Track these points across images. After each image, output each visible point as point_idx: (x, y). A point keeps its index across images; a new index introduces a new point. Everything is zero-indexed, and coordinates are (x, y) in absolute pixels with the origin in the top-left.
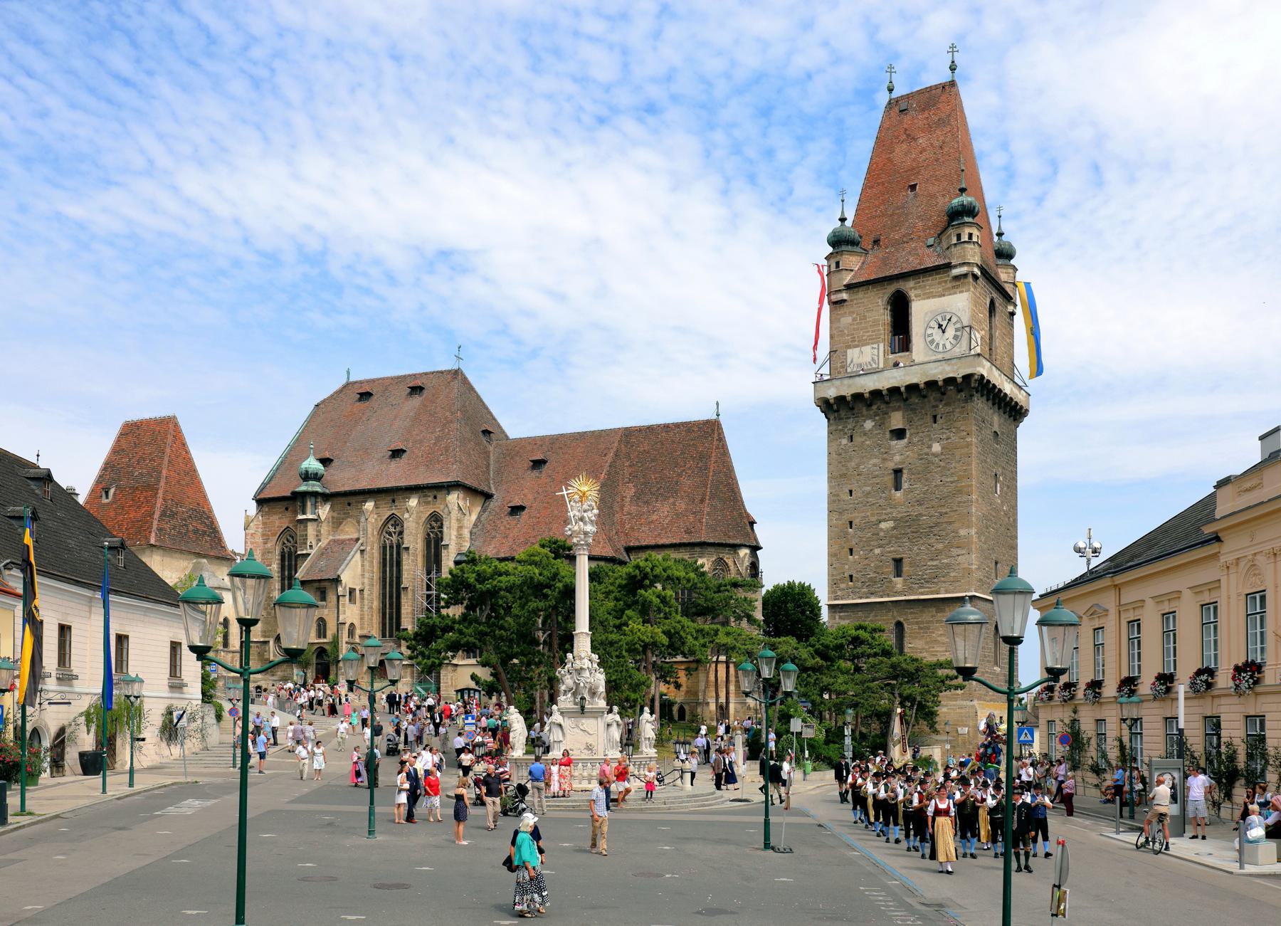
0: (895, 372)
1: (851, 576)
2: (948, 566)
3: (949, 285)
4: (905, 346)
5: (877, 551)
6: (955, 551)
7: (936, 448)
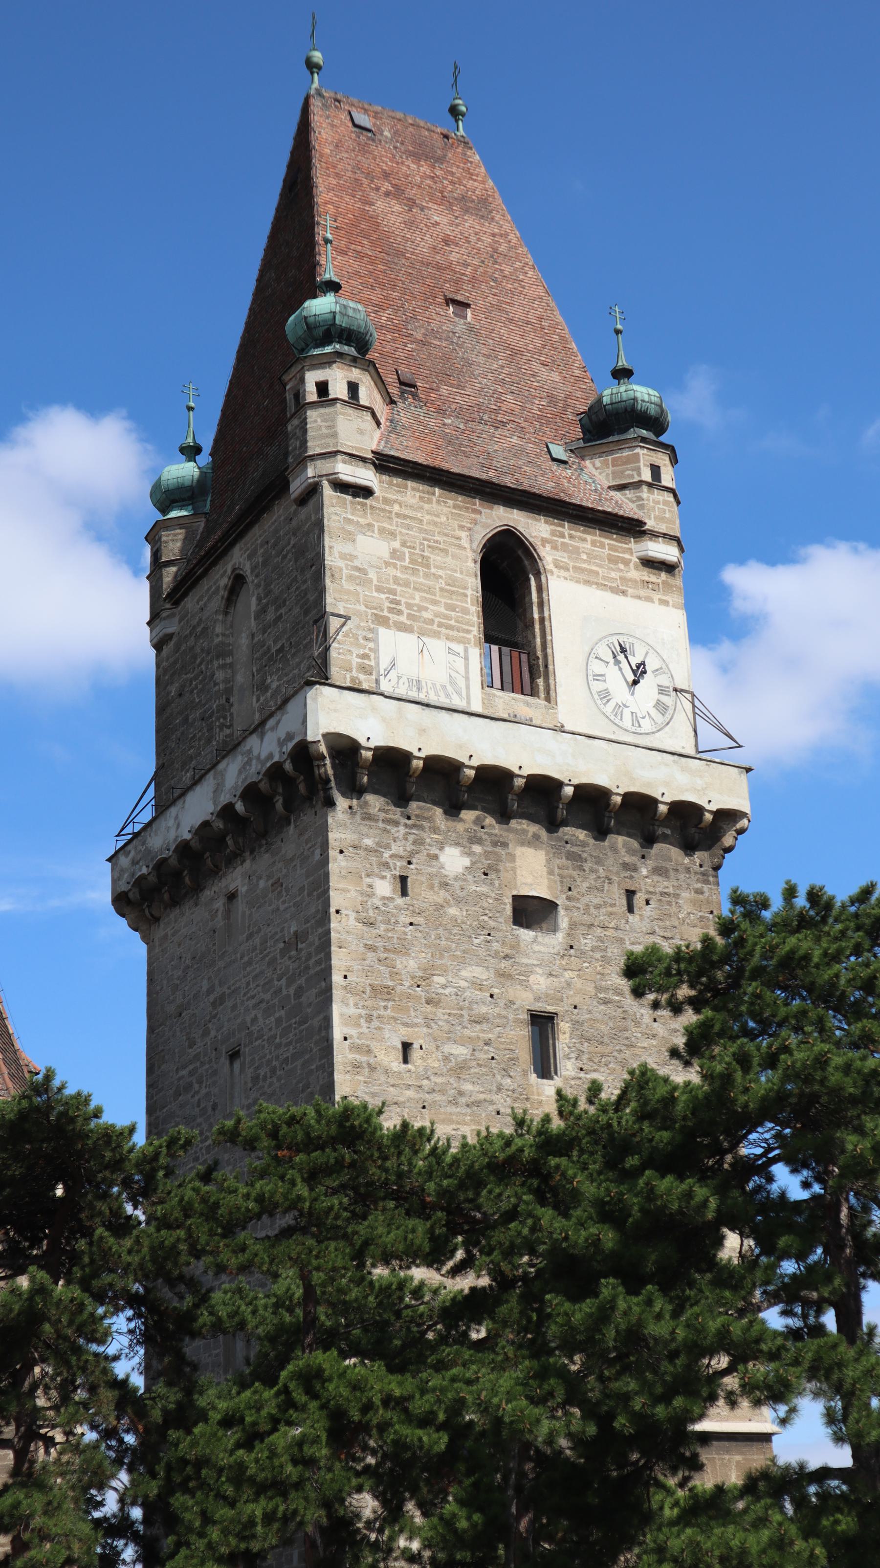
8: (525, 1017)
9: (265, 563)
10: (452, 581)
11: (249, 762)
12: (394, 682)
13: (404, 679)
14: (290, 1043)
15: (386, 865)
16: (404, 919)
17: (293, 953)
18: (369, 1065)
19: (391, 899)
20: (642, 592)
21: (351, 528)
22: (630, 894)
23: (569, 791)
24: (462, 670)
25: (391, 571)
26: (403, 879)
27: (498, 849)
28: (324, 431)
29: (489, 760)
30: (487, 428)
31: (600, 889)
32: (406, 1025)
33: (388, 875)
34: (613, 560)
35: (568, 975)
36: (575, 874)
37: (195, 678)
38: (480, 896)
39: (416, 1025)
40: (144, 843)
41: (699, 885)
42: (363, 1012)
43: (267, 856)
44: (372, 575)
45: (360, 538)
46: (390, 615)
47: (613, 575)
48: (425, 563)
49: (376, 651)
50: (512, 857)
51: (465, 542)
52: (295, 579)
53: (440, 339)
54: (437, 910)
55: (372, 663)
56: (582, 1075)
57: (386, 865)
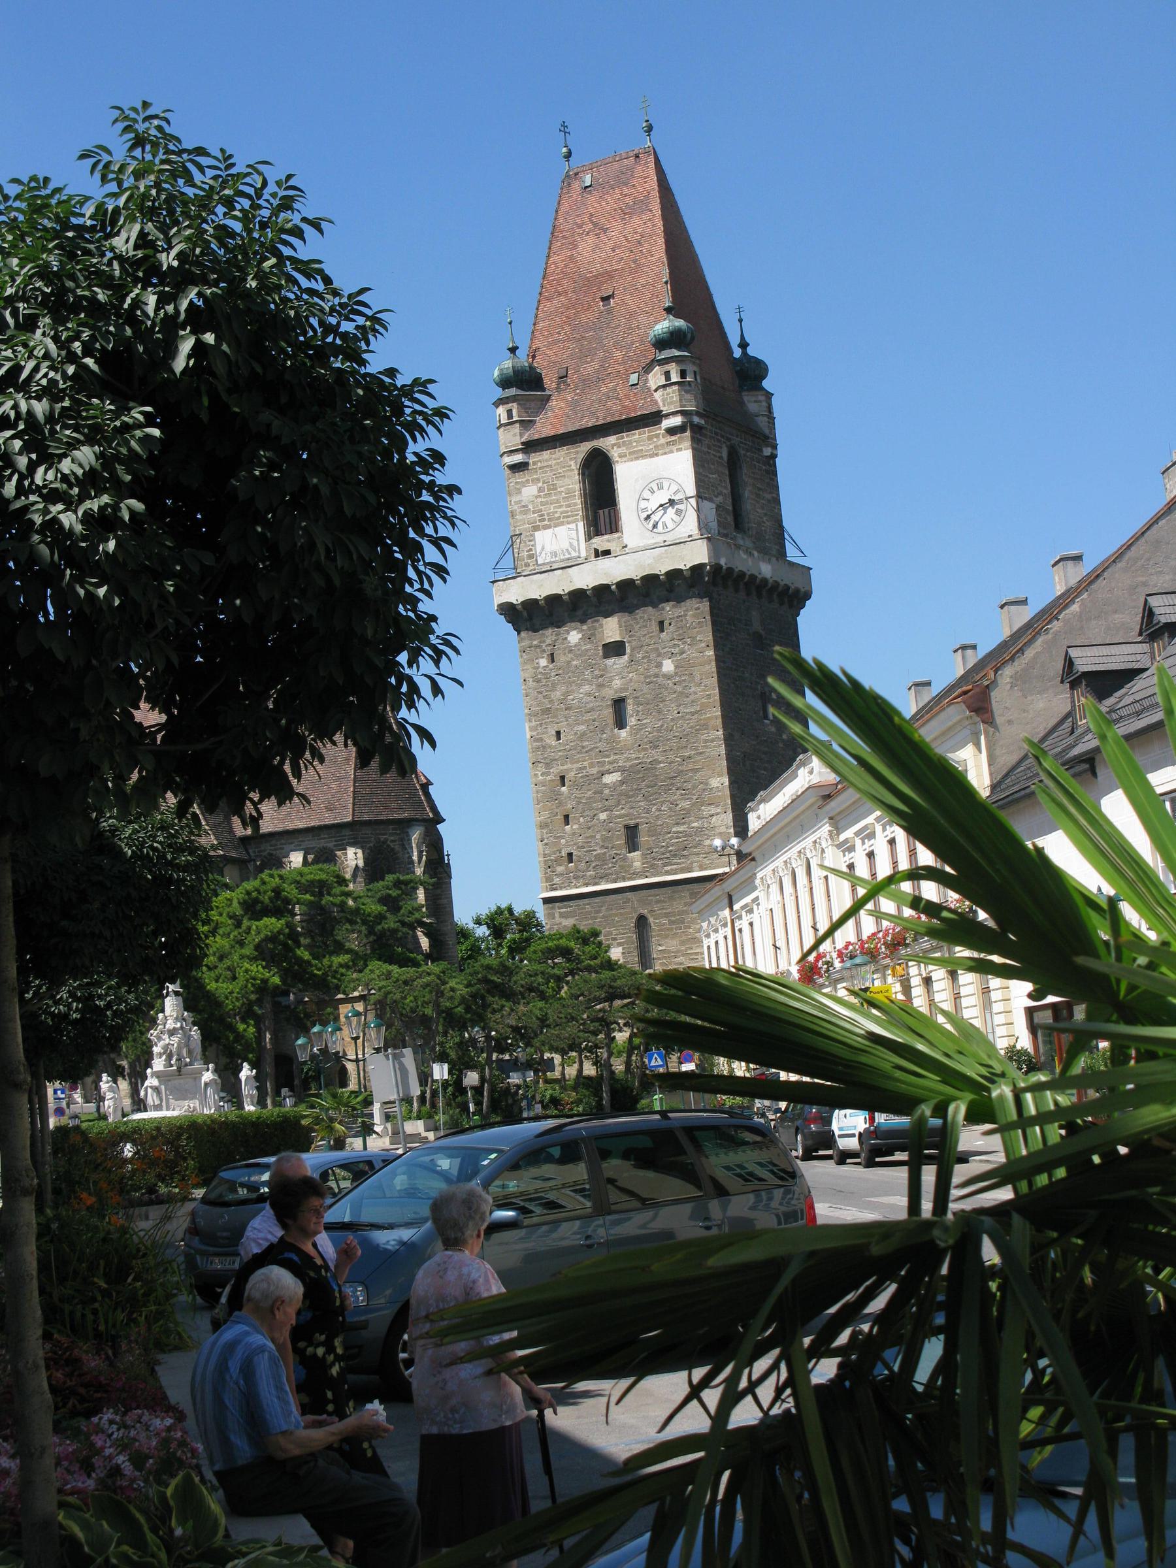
0: (605, 563)
1: (570, 855)
2: (700, 830)
3: (662, 441)
4: (614, 526)
5: (603, 816)
6: (706, 810)
7: (668, 666)
10: (568, 492)
15: (544, 651)
20: (667, 450)
22: (661, 623)
23: (613, 587)
25: (539, 500)
26: (552, 654)
34: (650, 438)
44: (530, 507)
45: (524, 490)
48: (554, 487)
50: (601, 626)
51: (573, 467)
57: (544, 651)
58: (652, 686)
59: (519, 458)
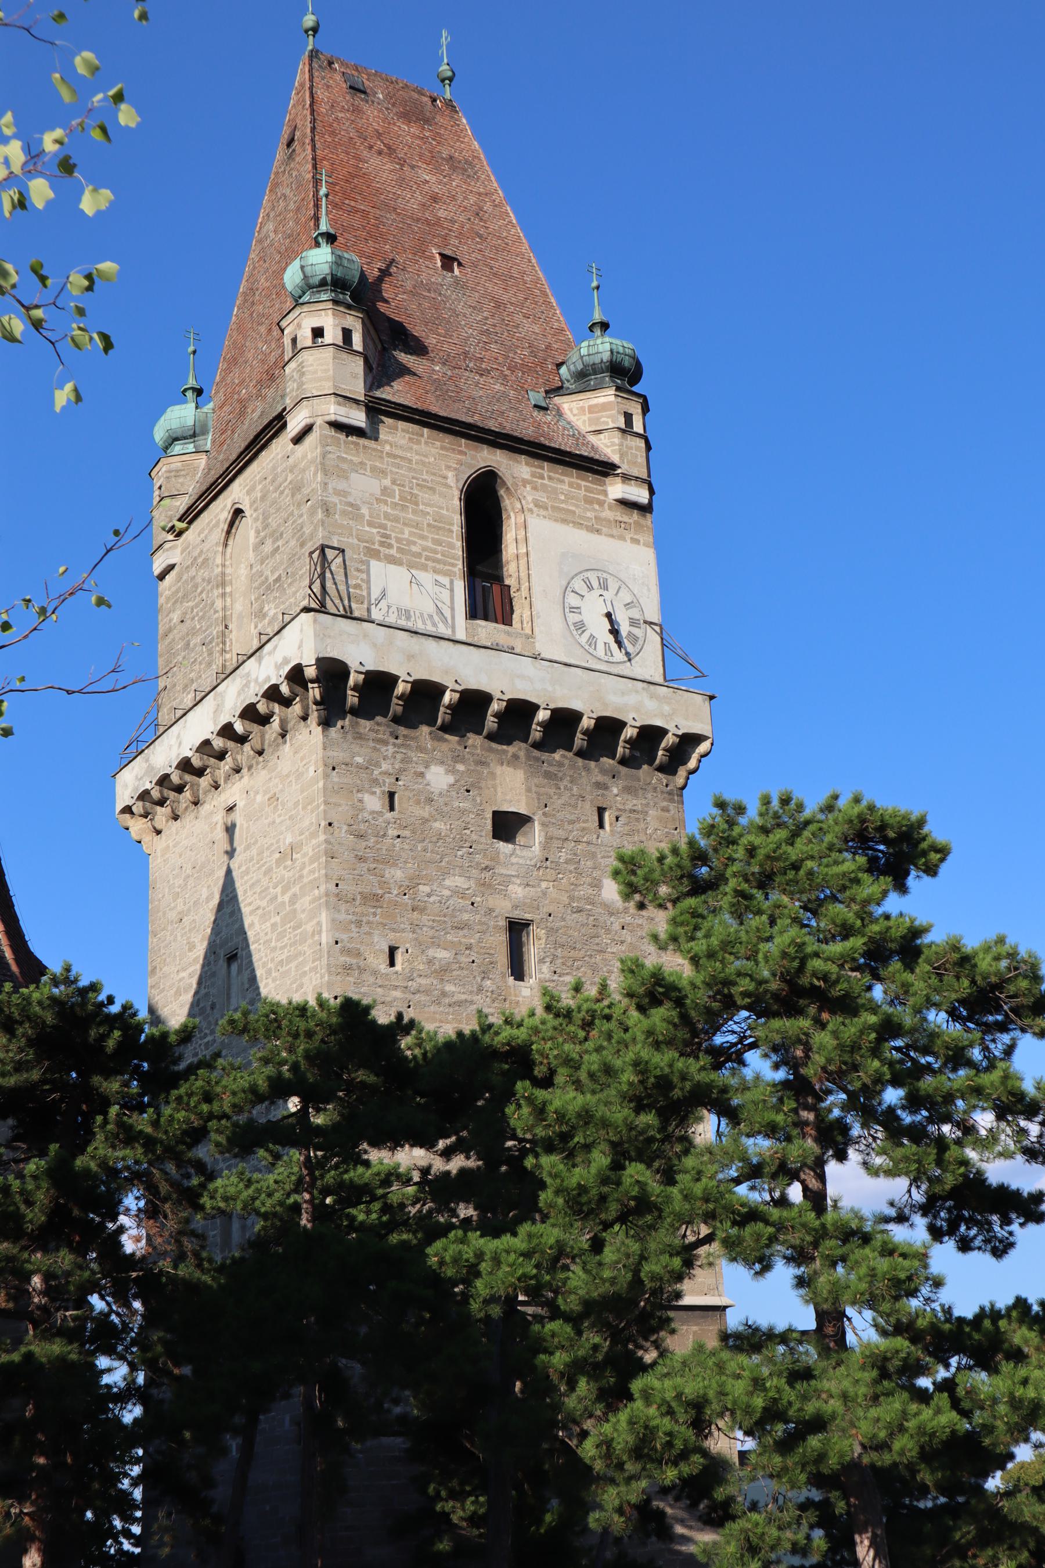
3: (607, 514)
8: (503, 923)
9: (263, 498)
10: (438, 518)
11: (247, 685)
12: (384, 611)
13: (394, 609)
14: (285, 946)
15: (375, 782)
16: (392, 832)
17: (289, 863)
18: (359, 967)
19: (380, 813)
20: (615, 532)
21: (345, 466)
22: (601, 811)
24: (448, 603)
26: (391, 795)
27: (479, 768)
28: (320, 374)
29: (473, 684)
30: (472, 375)
31: (575, 807)
32: (394, 930)
33: (378, 790)
34: (589, 501)
35: (544, 885)
36: (552, 791)
37: (197, 606)
38: (463, 812)
39: (403, 931)
40: (147, 760)
41: (665, 804)
42: (354, 918)
43: (264, 772)
44: (364, 511)
46: (382, 549)
47: (589, 514)
48: (414, 500)
49: (368, 582)
50: (493, 775)
51: (451, 480)
52: (292, 514)
53: (429, 291)
54: (423, 823)
55: (365, 593)
56: (556, 977)
57: (375, 782)
58: (581, 918)
59: (358, 418)
